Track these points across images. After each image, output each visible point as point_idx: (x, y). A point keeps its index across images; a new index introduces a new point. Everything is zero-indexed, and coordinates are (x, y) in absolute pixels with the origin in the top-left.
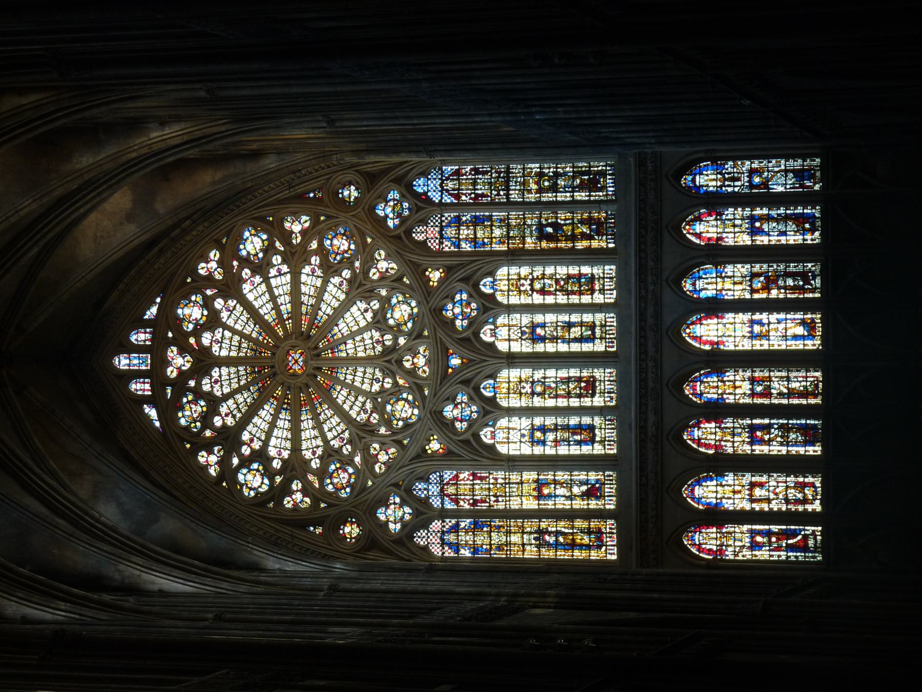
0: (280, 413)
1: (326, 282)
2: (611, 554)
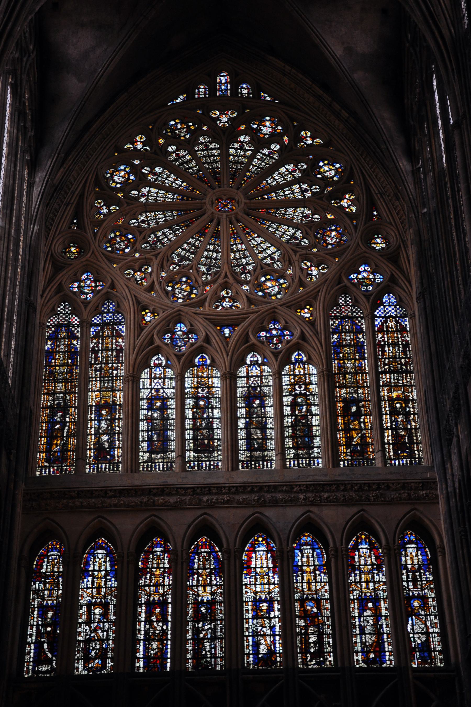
0: (179, 195)
1: (297, 227)
2: (41, 472)
